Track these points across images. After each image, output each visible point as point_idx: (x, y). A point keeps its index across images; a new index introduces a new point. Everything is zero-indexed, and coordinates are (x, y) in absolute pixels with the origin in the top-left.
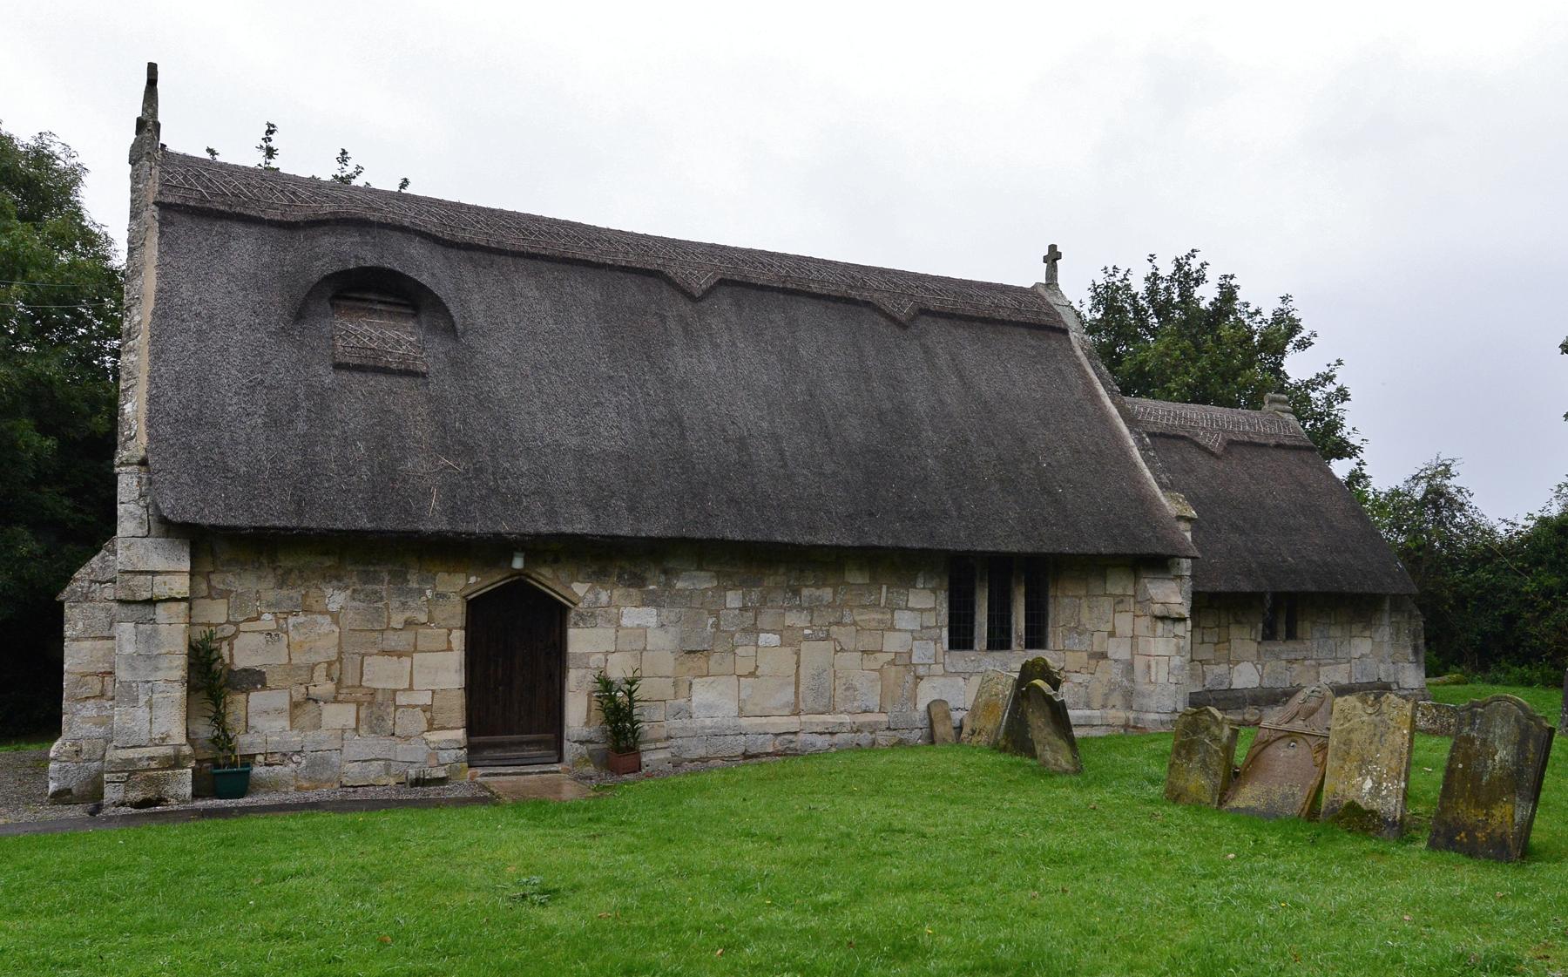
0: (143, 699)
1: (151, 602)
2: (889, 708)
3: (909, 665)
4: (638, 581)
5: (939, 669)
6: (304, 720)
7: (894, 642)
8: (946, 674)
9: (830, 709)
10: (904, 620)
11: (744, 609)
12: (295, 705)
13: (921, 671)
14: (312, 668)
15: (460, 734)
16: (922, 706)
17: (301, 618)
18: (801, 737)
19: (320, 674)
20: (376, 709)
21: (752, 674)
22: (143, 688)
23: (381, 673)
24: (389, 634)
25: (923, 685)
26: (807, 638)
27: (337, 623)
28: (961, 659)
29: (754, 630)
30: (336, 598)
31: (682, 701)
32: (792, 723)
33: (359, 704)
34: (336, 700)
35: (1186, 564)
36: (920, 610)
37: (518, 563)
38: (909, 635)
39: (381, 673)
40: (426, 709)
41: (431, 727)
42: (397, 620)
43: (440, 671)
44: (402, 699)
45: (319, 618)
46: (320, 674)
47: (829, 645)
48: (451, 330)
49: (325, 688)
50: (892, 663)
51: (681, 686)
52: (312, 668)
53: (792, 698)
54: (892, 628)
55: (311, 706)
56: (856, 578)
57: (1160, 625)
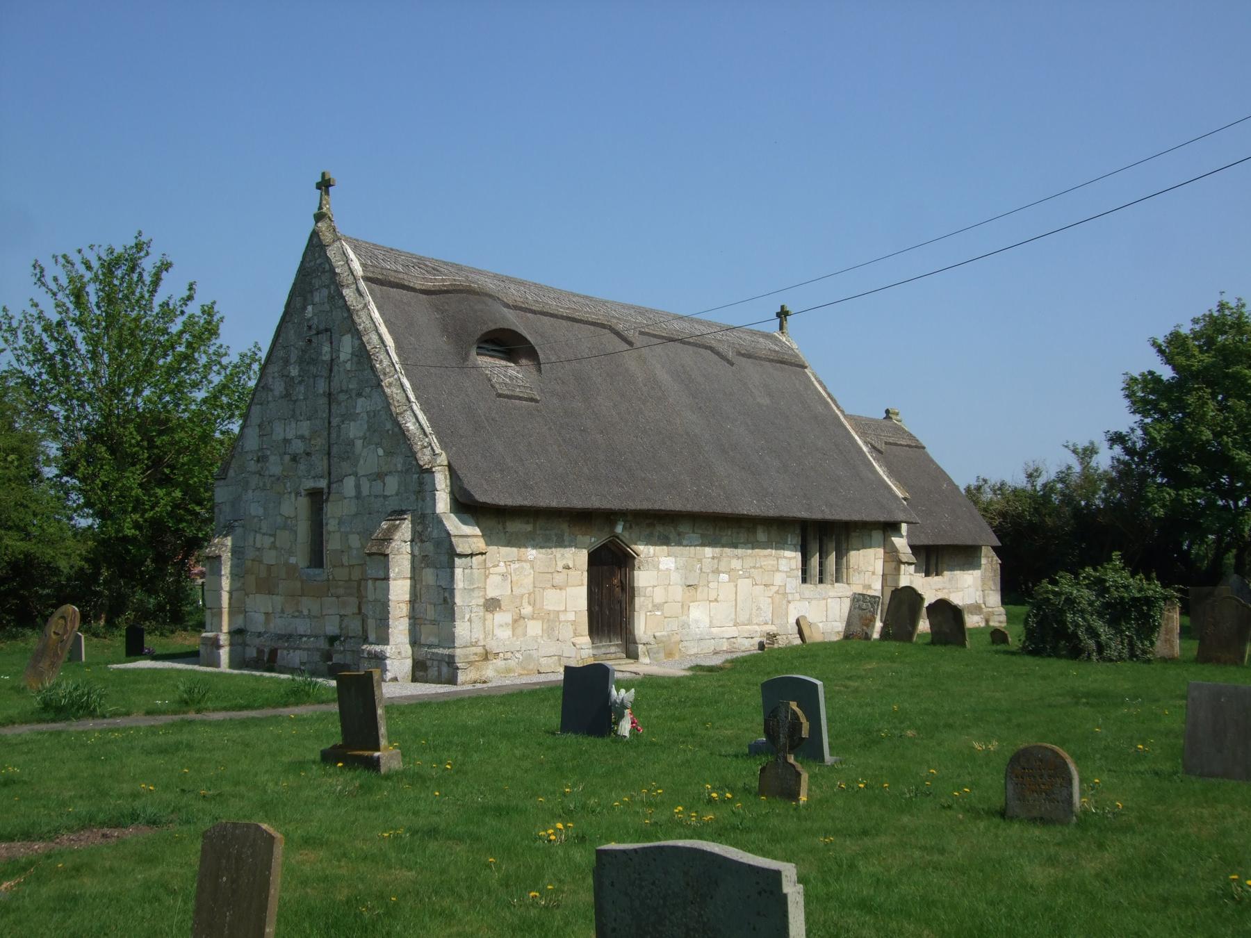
0: (467, 617)
1: (472, 555)
2: (776, 622)
3: (785, 594)
4: (665, 541)
5: (797, 596)
6: (519, 631)
7: (779, 579)
8: (802, 599)
9: (750, 623)
10: (784, 566)
11: (713, 558)
12: (515, 621)
13: (790, 598)
14: (522, 596)
15: (587, 639)
16: (792, 621)
17: (517, 565)
18: (739, 640)
19: (525, 600)
20: (551, 621)
21: (716, 600)
22: (468, 610)
23: (552, 600)
24: (555, 574)
25: (791, 606)
26: (741, 577)
27: (533, 567)
28: (809, 589)
29: (717, 572)
30: (531, 553)
31: (684, 618)
32: (732, 631)
33: (543, 620)
34: (533, 618)
35: (904, 527)
36: (790, 559)
37: (619, 529)
38: (784, 575)
39: (552, 600)
40: (573, 623)
41: (576, 635)
42: (560, 564)
43: (573, 598)
44: (562, 617)
45: (524, 564)
46: (525, 600)
47: (748, 581)
48: (539, 370)
49: (527, 610)
50: (777, 592)
51: (685, 607)
52: (522, 596)
53: (733, 616)
54: (778, 570)
55: (522, 621)
56: (761, 536)
57: (903, 567)
